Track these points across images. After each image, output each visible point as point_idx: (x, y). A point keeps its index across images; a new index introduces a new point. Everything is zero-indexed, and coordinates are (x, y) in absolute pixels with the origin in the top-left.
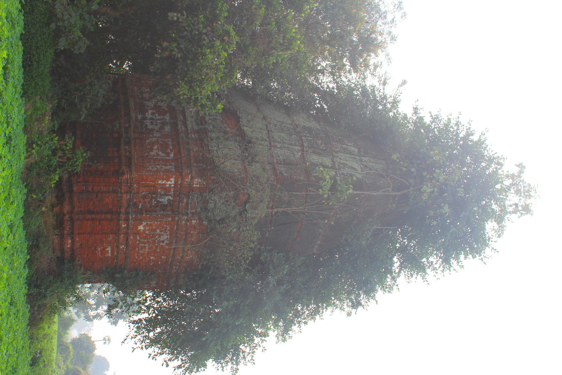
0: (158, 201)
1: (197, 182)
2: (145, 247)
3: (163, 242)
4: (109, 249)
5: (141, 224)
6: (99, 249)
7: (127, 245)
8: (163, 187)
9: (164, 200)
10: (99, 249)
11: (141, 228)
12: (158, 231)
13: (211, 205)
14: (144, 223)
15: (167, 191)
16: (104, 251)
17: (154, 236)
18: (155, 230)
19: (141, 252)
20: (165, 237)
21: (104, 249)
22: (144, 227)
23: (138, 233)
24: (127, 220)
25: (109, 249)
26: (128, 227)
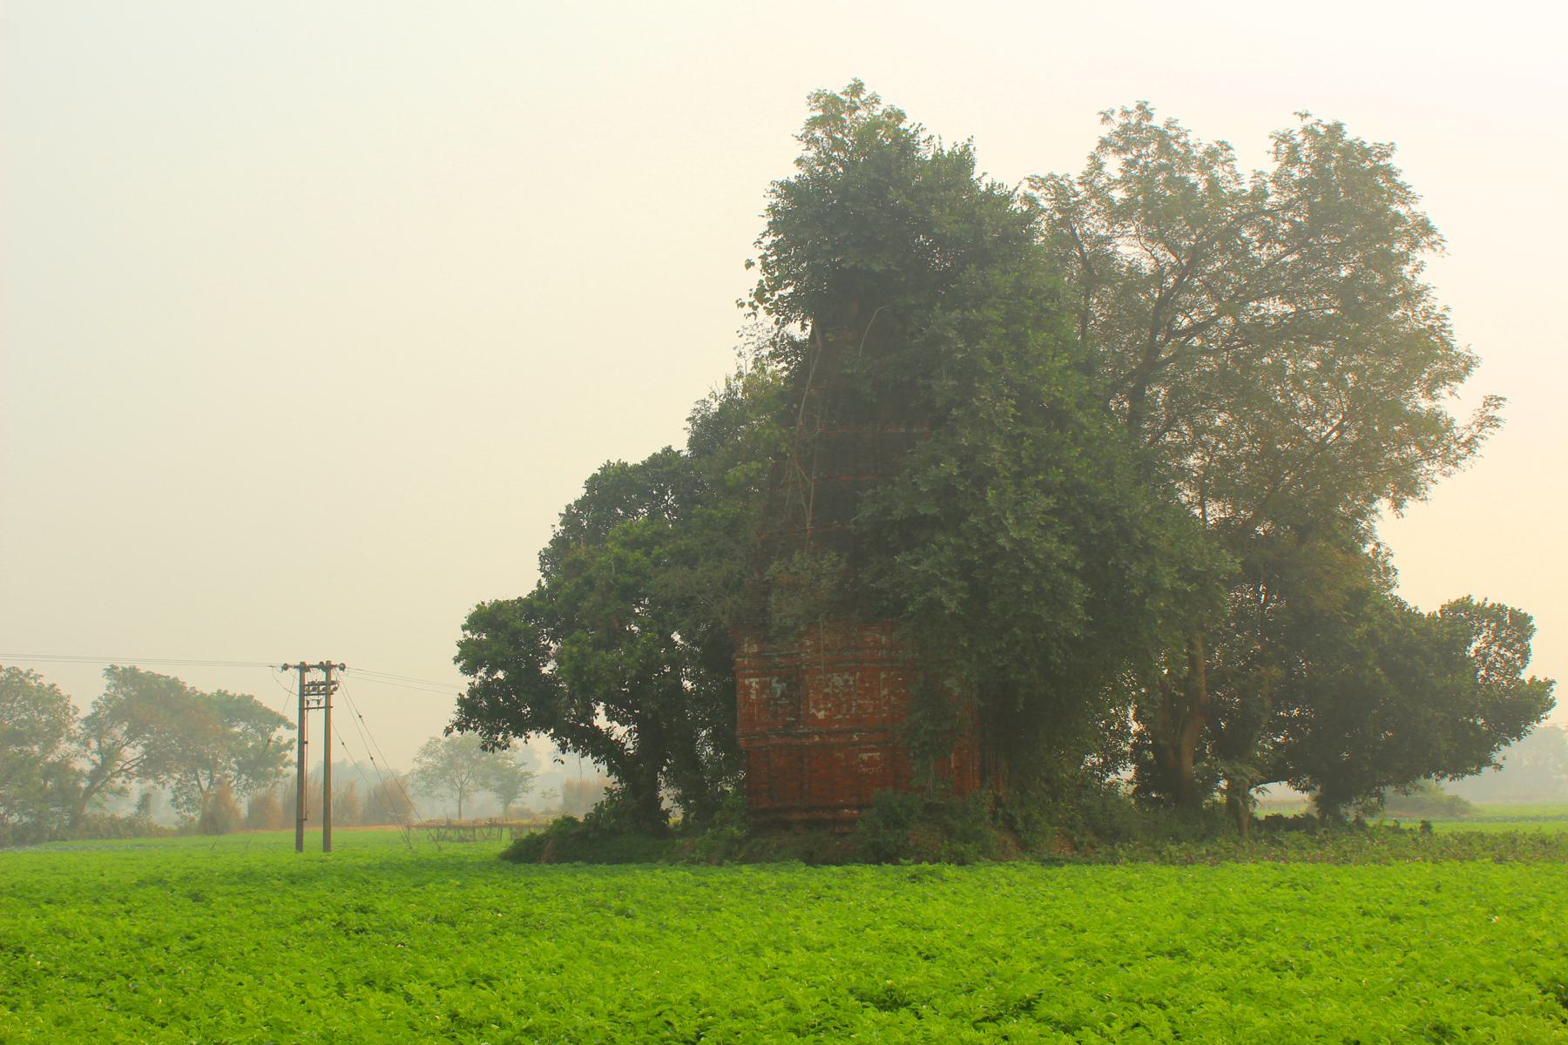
0: (783, 694)
2: (859, 706)
4: (865, 756)
5: (814, 716)
6: (865, 770)
7: (851, 732)
9: (778, 688)
10: (865, 770)
11: (821, 715)
13: (789, 622)
14: (813, 711)
15: (764, 686)
16: (870, 763)
17: (836, 695)
18: (827, 695)
20: (837, 680)
21: (863, 762)
23: (828, 719)
24: (807, 735)
25: (865, 756)
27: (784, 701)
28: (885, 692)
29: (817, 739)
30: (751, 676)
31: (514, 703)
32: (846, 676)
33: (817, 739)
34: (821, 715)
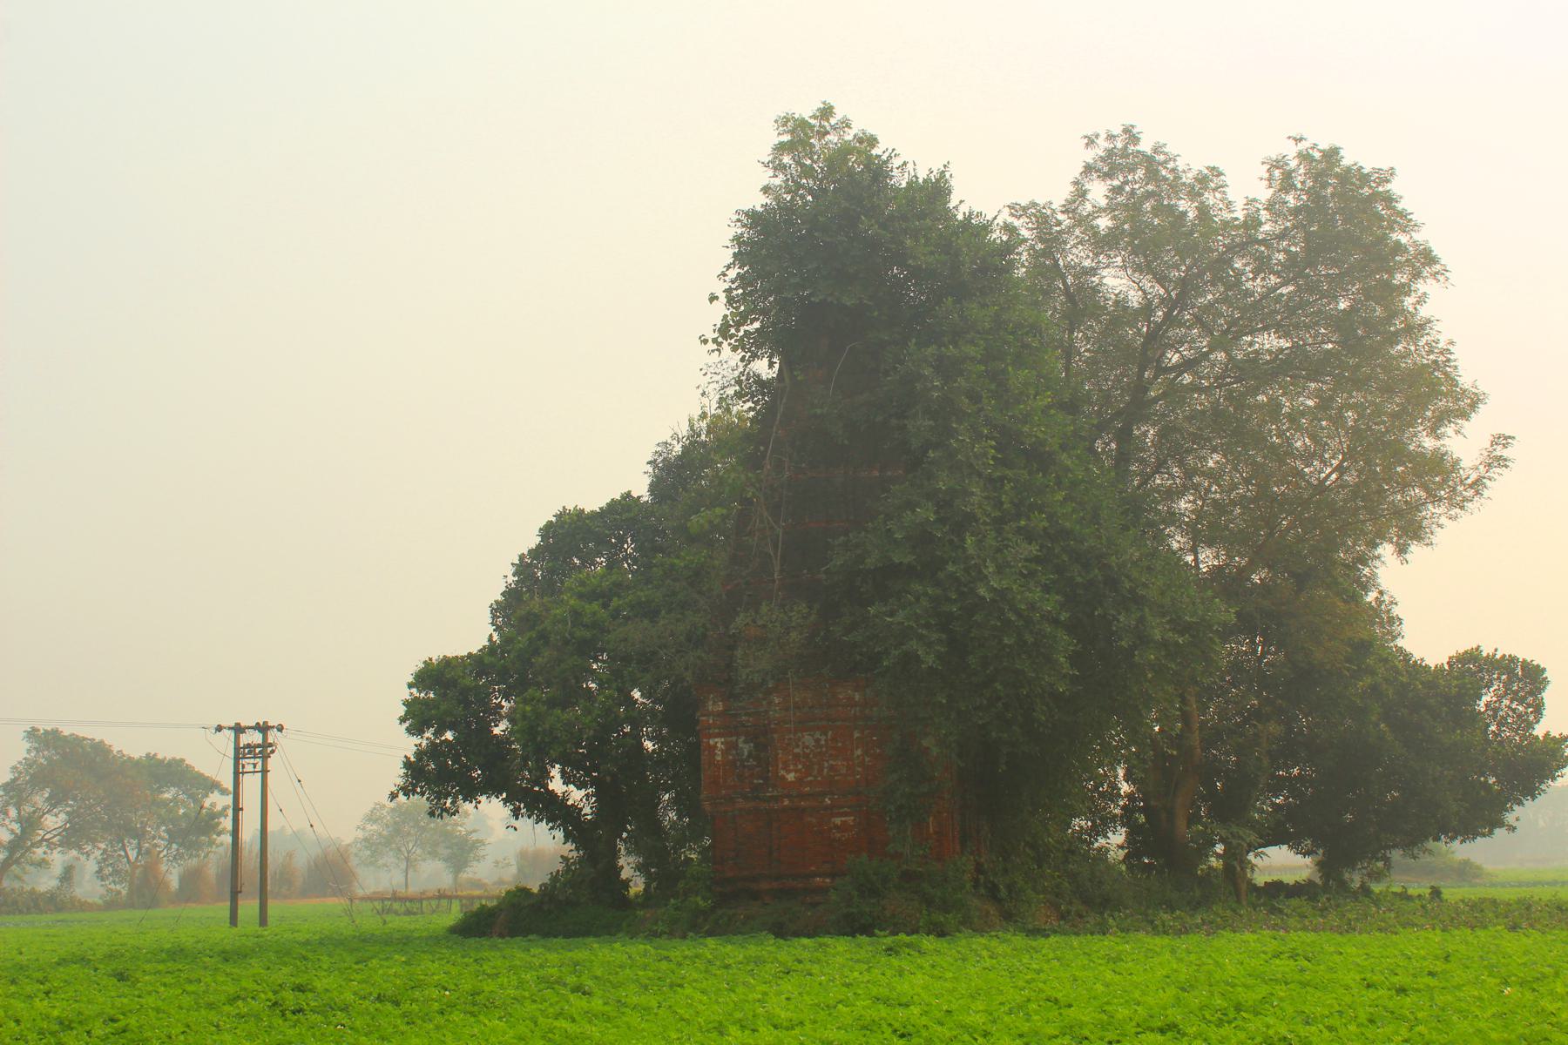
0: (750, 755)
1: (715, 706)
2: (832, 768)
3: (817, 741)
4: (838, 821)
5: (783, 777)
8: (724, 753)
9: (746, 748)
11: (791, 777)
12: (797, 750)
13: (757, 678)
15: (731, 747)
16: (843, 828)
18: (796, 756)
19: (844, 771)
20: (808, 739)
21: (836, 827)
22: (789, 772)
23: (800, 781)
24: (776, 799)
25: (838, 821)
26: (788, 796)
27: (752, 762)
28: (859, 752)
29: (786, 802)
30: (719, 735)
31: (463, 766)
32: (817, 735)
33: (786, 802)
34: (791, 777)
